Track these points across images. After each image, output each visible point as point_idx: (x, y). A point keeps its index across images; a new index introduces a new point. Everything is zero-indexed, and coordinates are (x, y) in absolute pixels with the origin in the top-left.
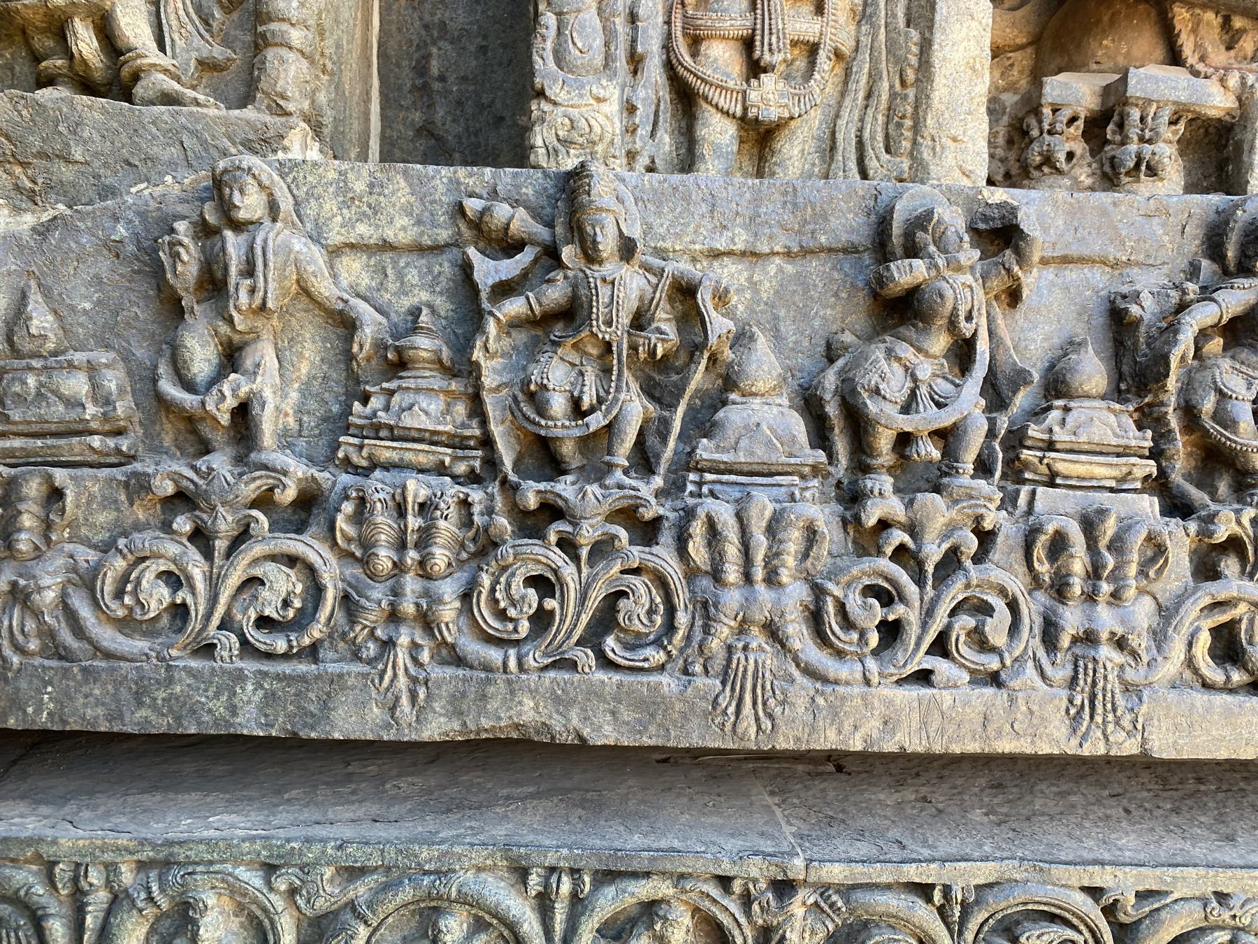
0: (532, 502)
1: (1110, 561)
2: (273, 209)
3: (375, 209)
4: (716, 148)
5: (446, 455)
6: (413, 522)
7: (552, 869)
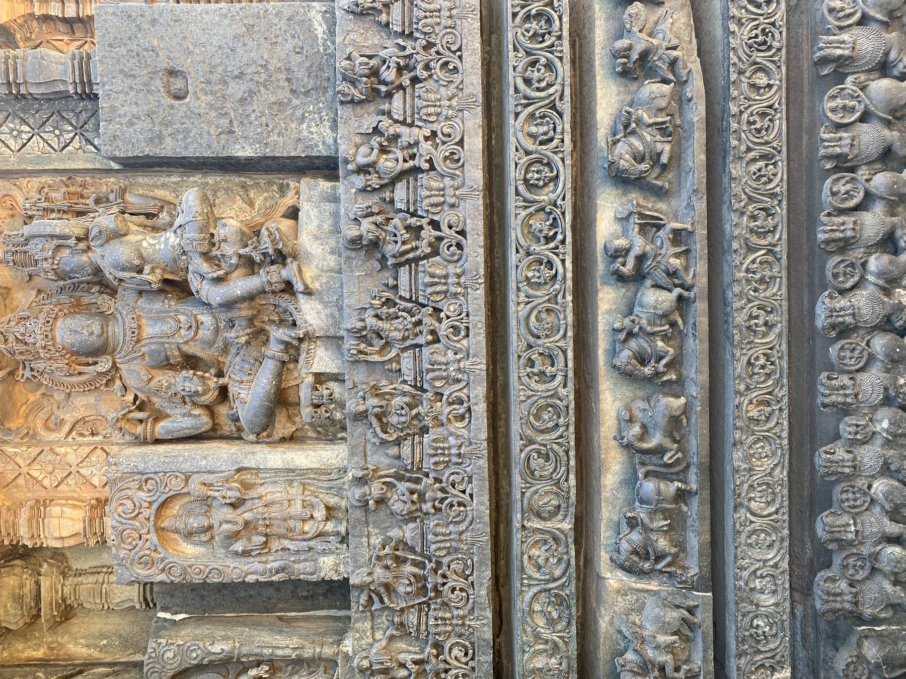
0: (433, 594)
1: (439, 451)
2: (365, 657)
3: (363, 631)
4: (334, 527)
5: (423, 614)
6: (440, 622)
7: (522, 584)
